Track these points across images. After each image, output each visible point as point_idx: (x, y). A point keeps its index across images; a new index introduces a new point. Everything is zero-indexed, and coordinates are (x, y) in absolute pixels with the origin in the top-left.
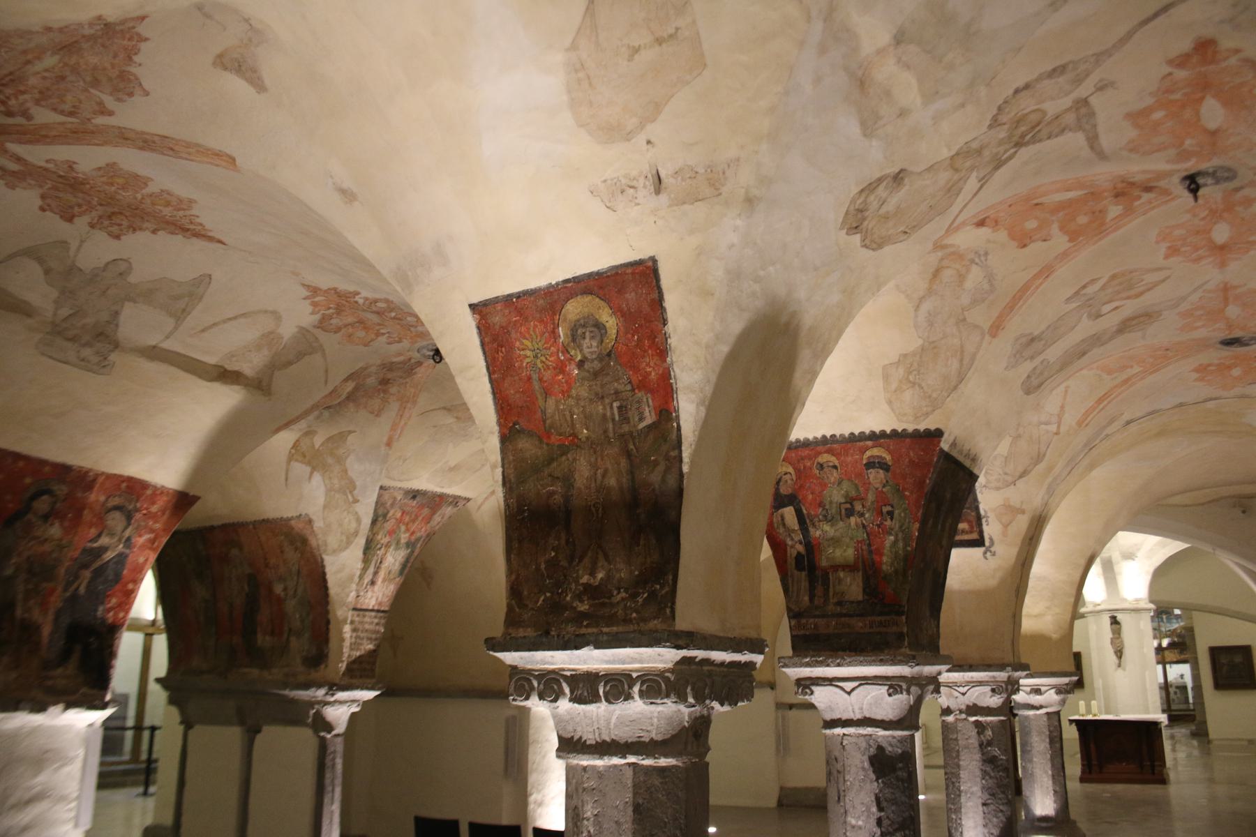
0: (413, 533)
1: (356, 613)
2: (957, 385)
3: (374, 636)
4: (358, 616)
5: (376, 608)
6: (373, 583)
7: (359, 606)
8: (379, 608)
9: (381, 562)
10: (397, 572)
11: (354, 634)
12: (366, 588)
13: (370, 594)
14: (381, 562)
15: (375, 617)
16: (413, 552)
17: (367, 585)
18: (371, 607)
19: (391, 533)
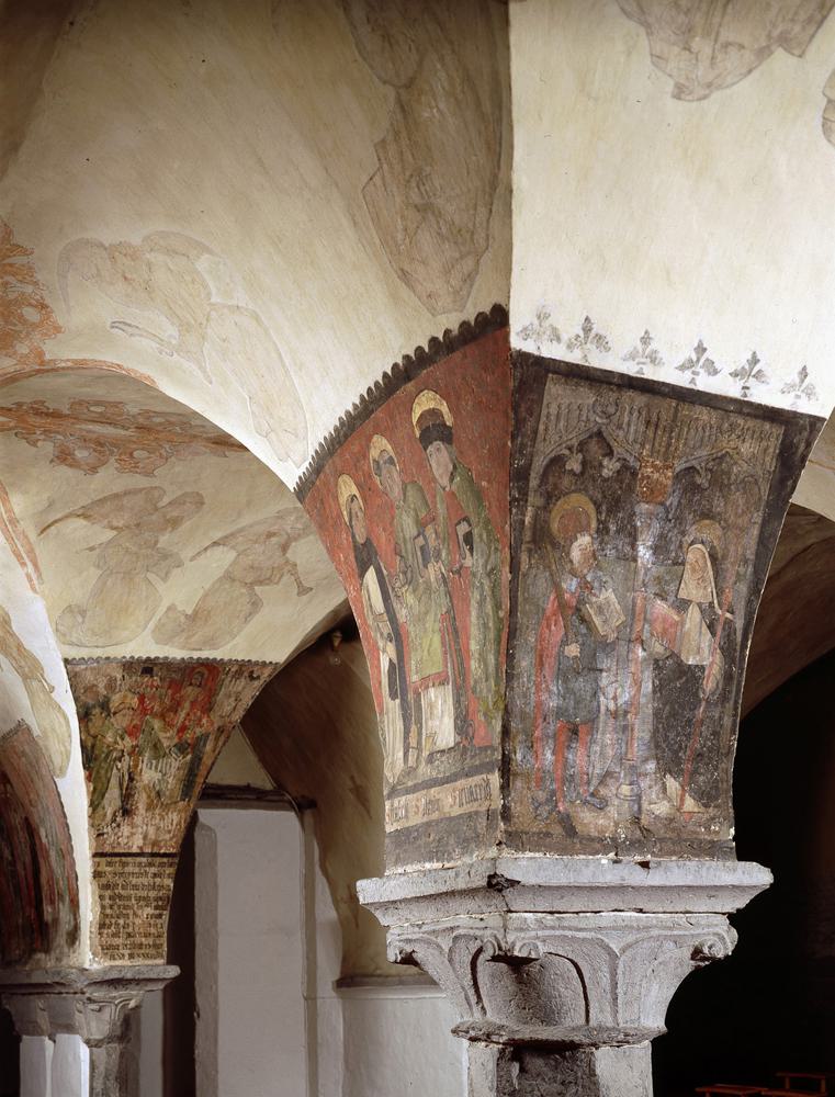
0: (183, 729)
1: (104, 860)
2: (495, 176)
3: (152, 894)
4: (109, 864)
5: (148, 850)
6: (127, 812)
7: (108, 849)
8: (156, 850)
9: (131, 779)
10: (178, 793)
11: (108, 893)
12: (114, 821)
13: (126, 830)
14: (131, 779)
15: (151, 865)
16: (200, 759)
17: (114, 815)
18: (135, 850)
19: (132, 731)
